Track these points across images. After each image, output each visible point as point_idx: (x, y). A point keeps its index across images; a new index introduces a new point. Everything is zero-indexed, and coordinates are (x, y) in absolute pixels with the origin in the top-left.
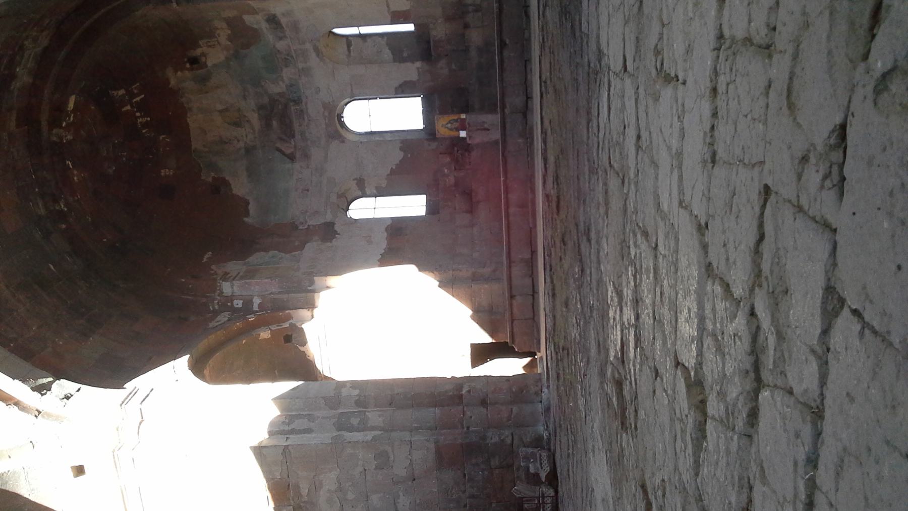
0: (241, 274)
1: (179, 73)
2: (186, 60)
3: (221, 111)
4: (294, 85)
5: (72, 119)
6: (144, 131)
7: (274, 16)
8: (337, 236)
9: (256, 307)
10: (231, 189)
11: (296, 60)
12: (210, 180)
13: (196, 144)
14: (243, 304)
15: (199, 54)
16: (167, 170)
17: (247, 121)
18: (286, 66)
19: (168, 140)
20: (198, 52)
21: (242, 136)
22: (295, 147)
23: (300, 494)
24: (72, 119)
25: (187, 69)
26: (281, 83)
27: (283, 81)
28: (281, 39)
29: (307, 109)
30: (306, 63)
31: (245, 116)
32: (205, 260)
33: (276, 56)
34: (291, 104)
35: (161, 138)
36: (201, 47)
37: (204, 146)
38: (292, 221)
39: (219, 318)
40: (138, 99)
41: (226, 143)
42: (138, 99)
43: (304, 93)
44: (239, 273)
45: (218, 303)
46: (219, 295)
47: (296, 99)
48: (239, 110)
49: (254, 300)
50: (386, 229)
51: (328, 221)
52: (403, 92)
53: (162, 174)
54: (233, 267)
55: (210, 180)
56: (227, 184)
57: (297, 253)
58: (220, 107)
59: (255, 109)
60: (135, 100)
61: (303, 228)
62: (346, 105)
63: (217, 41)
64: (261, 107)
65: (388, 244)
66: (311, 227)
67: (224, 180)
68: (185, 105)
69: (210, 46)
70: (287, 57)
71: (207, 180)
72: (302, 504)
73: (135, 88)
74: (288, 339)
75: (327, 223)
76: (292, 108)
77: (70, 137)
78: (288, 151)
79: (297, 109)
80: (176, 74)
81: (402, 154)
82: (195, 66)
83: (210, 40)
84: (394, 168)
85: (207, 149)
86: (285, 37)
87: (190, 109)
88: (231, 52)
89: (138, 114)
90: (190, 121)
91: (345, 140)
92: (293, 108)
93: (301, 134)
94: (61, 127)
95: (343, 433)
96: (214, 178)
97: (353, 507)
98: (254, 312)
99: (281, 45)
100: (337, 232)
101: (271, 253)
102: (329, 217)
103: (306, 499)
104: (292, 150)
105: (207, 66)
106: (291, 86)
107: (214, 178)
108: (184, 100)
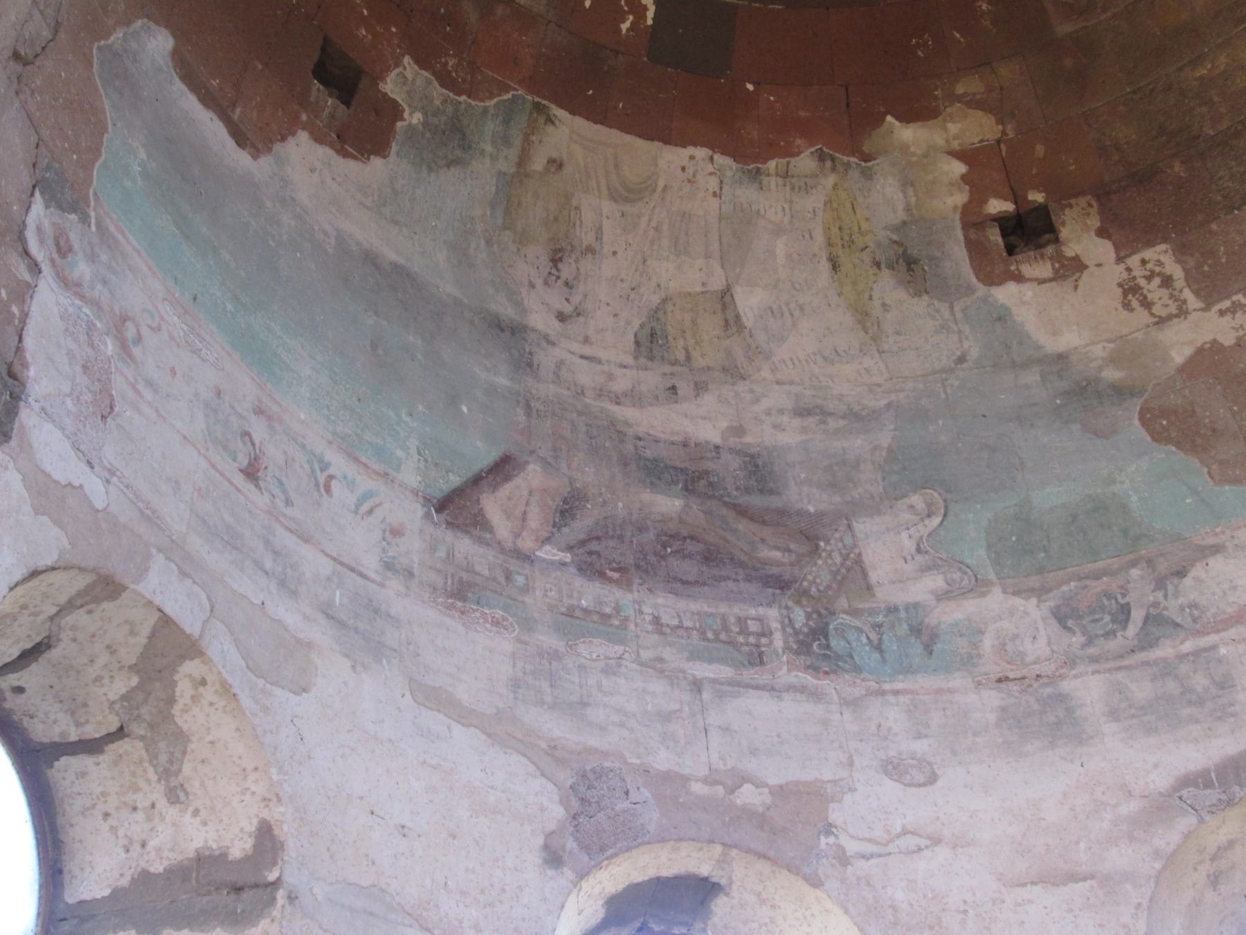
1: (959, 168)
2: (1037, 197)
3: (725, 297)
4: (929, 649)
10: (319, 139)
11: (1126, 662)
12: (390, 86)
15: (1069, 252)
17: (673, 388)
18: (1062, 617)
19: (625, 27)
21: (586, 340)
22: (526, 558)
26: (936, 581)
27: (941, 596)
30: (1113, 714)
31: (700, 388)
33: (1133, 564)
34: (799, 616)
36: (1120, 260)
37: (556, 164)
38: (93, 214)
41: (556, 260)
43: (882, 693)
55: (390, 86)
58: (749, 302)
59: (748, 439)
61: (31, 220)
68: (772, 164)
69: (1130, 290)
70: (1137, 615)
71: (392, 75)
76: (772, 615)
78: (493, 505)
80: (959, 155)
82: (995, 236)
83: (1179, 282)
85: (538, 164)
90: (692, 157)
91: (569, 873)
93: (605, 617)
105: (991, 280)
106: (916, 631)
107: (395, 111)
108: (805, 162)
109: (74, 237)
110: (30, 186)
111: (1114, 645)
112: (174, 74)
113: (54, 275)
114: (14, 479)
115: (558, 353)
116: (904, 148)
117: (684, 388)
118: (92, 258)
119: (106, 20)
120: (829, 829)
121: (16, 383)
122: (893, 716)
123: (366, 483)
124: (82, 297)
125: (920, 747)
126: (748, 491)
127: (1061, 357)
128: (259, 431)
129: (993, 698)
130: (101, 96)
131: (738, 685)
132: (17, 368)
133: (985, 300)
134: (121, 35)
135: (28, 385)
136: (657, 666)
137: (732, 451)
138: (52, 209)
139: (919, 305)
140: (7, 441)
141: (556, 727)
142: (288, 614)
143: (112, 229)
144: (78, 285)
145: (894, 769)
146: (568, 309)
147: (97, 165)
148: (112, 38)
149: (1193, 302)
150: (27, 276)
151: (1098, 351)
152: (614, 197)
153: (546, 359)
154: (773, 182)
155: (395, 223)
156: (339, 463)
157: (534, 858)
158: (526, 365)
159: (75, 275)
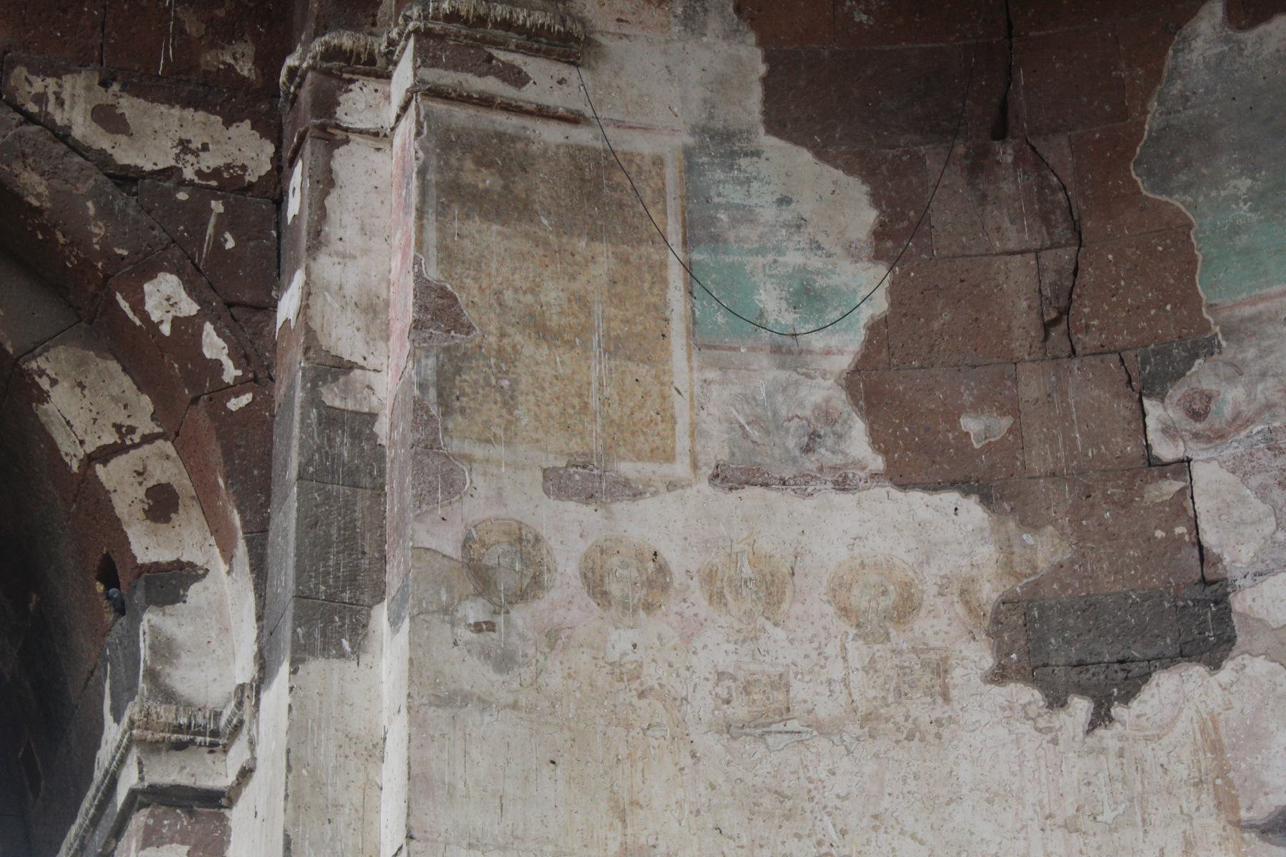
8: (1081, 707)
61: (1152, 436)
66: (1171, 487)
75: (1222, 601)
100: (1126, 698)
109: (1208, 384)
110: (1135, 406)
112: (1241, 35)
113: (1204, 446)
114: (1259, 666)
118: (1238, 369)
119: (1129, 120)
121: (1215, 587)
124: (1249, 422)
130: (1166, 203)
132: (1210, 573)
134: (1156, 104)
135: (1228, 575)
138: (1171, 391)
140: (1234, 644)
143: (1247, 311)
144: (1237, 415)
147: (1197, 277)
148: (1147, 127)
150: (1178, 485)
159: (1228, 411)
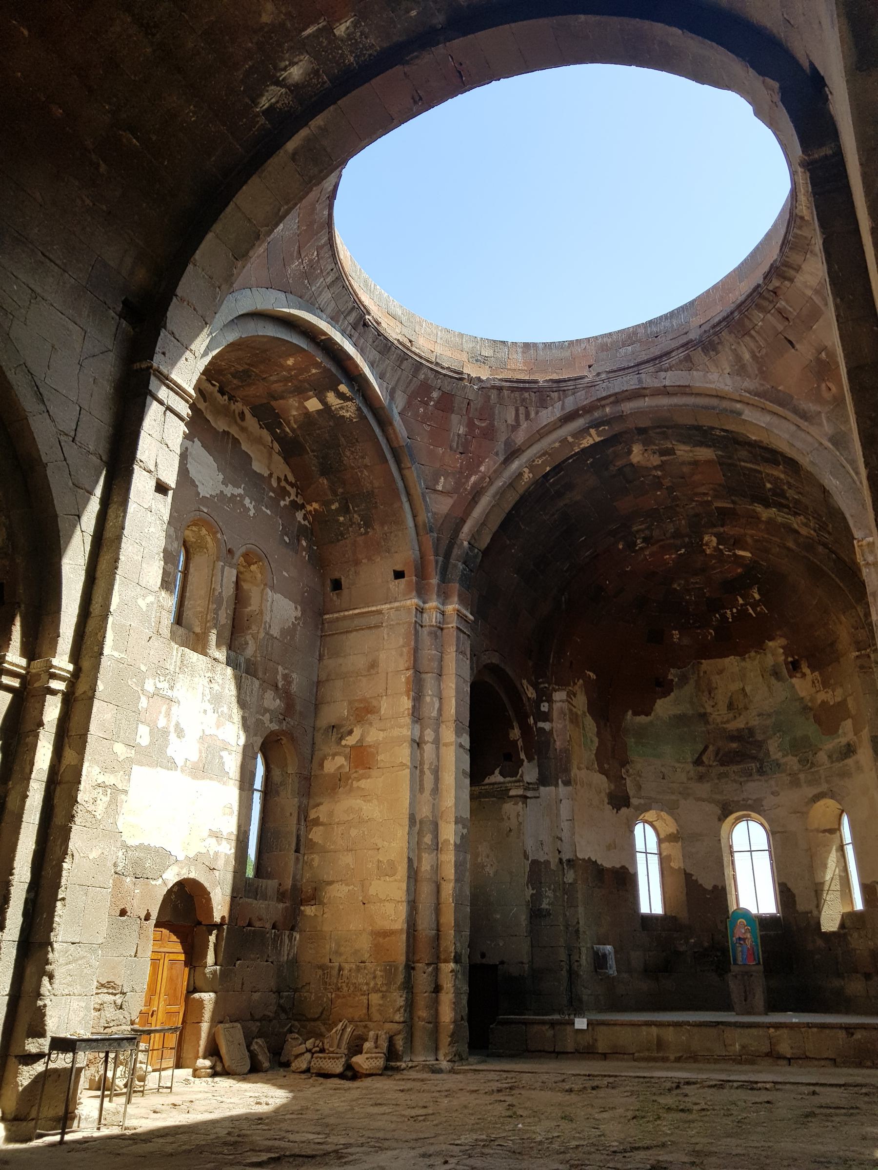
0: (574, 710)
1: (782, 651)
2: (796, 657)
3: (743, 689)
5: (727, 553)
6: (717, 616)
7: (854, 752)
8: (615, 810)
9: (541, 724)
10: (660, 699)
12: (670, 677)
13: (706, 665)
14: (544, 712)
16: (678, 636)
17: (735, 716)
20: (807, 670)
21: (718, 710)
23: (359, 780)
24: (727, 553)
25: (786, 658)
26: (780, 754)
28: (830, 757)
29: (754, 781)
30: (805, 782)
31: (740, 714)
32: (588, 673)
34: (758, 765)
35: (711, 631)
39: (531, 688)
40: (751, 611)
42: (751, 611)
44: (575, 707)
45: (546, 687)
46: (553, 688)
47: (764, 770)
48: (746, 708)
49: (548, 723)
50: (623, 867)
51: (631, 801)
52: (781, 892)
53: (674, 632)
54: (581, 701)
55: (670, 677)
56: (665, 694)
57: (596, 766)
58: (748, 689)
60: (749, 608)
62: (762, 824)
63: (820, 691)
64: (751, 731)
65: (608, 870)
67: (672, 691)
69: (813, 682)
70: (810, 762)
72: (350, 781)
73: (762, 609)
74: (508, 757)
77: (708, 552)
78: (705, 758)
79: (752, 769)
80: (780, 647)
81: (709, 887)
84: (693, 878)
85: (702, 674)
86: (832, 762)
87: (744, 659)
88: (810, 704)
89: (735, 610)
92: (753, 766)
94: (718, 544)
95: (418, 826)
96: (672, 680)
97: (342, 834)
98: (536, 723)
99: (822, 756)
101: (596, 740)
102: (634, 801)
103: (355, 784)
104: (707, 763)
105: (791, 677)
107: (672, 680)
108: (753, 654)
111: (806, 767)
114: (632, 810)
115: (713, 716)
116: (771, 647)
117: (737, 715)
118: (631, 768)
120: (762, 806)
122: (772, 782)
123: (682, 766)
125: (777, 789)
126: (749, 738)
127: (802, 698)
128: (663, 770)
129: (789, 778)
131: (747, 781)
133: (791, 682)
136: (735, 781)
137: (747, 728)
139: (780, 683)
141: (718, 797)
142: (674, 797)
145: (773, 793)
146: (714, 704)
149: (822, 689)
151: (808, 698)
152: (718, 674)
153: (711, 720)
154: (748, 660)
155: (678, 704)
156: (677, 765)
157: (717, 820)
158: (707, 723)
